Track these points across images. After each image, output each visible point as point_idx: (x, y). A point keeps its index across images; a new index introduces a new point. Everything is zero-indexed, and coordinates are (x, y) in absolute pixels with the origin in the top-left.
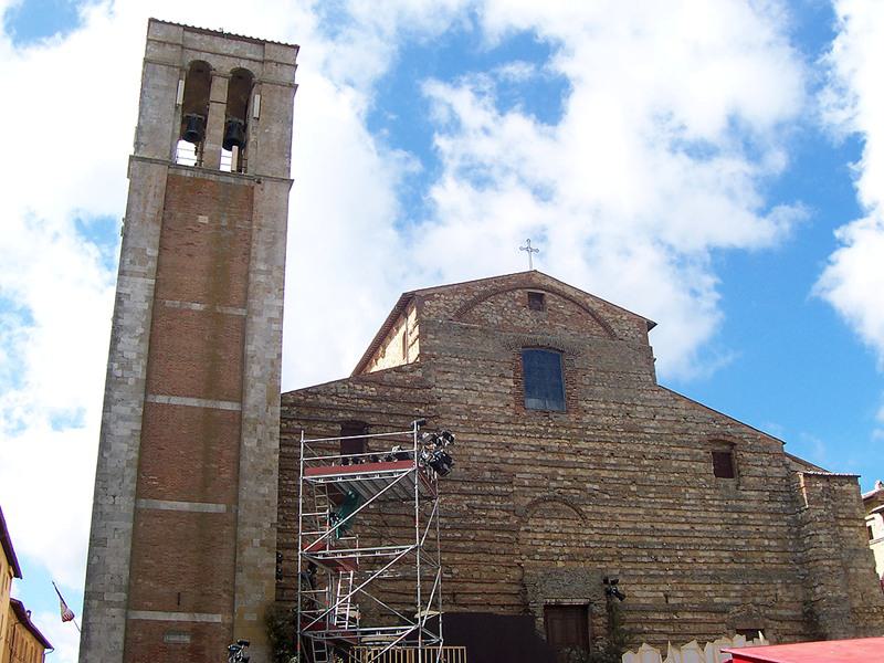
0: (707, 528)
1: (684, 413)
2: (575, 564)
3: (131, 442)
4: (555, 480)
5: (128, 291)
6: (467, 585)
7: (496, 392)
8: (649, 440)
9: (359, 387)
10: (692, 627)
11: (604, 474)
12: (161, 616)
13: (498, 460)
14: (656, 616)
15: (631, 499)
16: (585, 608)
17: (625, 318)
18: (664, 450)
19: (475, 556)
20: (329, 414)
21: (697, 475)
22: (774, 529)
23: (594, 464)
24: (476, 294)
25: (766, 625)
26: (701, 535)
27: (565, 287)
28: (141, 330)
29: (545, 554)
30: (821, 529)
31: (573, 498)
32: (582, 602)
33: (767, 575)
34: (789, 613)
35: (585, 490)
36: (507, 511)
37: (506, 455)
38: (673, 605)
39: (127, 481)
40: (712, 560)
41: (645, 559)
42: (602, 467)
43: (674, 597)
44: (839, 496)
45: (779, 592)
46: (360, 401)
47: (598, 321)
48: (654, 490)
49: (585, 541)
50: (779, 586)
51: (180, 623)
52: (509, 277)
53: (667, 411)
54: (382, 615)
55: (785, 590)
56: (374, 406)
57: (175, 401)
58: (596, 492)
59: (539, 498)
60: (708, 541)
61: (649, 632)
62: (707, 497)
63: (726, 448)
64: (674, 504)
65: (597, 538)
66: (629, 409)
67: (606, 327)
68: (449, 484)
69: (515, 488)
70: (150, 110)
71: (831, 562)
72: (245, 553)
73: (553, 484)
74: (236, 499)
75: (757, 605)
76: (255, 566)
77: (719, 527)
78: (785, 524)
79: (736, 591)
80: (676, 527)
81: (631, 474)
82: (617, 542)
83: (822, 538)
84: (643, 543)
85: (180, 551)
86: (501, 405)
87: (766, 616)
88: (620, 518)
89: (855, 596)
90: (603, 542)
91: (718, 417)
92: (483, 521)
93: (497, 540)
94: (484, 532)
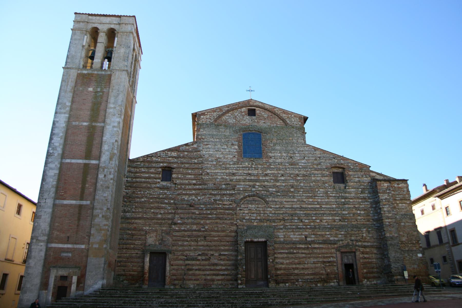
0: (328, 206)
1: (319, 156)
2: (262, 224)
3: (54, 178)
4: (254, 187)
5: (57, 120)
6: (212, 233)
7: (229, 151)
8: (301, 168)
9: (169, 153)
10: (318, 251)
11: (278, 184)
12: (61, 246)
13: (229, 180)
14: (301, 246)
15: (290, 195)
16: (265, 242)
17: (293, 116)
18: (308, 173)
19: (216, 221)
20: (157, 165)
21: (324, 183)
23: (273, 180)
24: (224, 111)
25: (356, 250)
26: (325, 209)
27: (265, 105)
28: (61, 134)
29: (248, 219)
30: (385, 205)
31: (262, 195)
32: (263, 240)
33: (357, 227)
34: (369, 244)
35: (268, 191)
36: (232, 201)
37: (232, 178)
38: (309, 241)
39: (51, 193)
40: (330, 221)
41: (296, 221)
42: (277, 181)
43: (310, 237)
44: (397, 189)
45: (364, 235)
46: (170, 159)
47: (280, 118)
48: (302, 190)
49: (267, 214)
51: (68, 248)
52: (239, 103)
53: (310, 155)
54: (173, 246)
55: (367, 233)
56: (176, 160)
57: (73, 161)
59: (247, 196)
60: (328, 212)
61: (297, 253)
62: (329, 193)
63: (340, 170)
64: (312, 196)
65: (273, 212)
66: (292, 155)
67: (284, 120)
70: (72, 49)
71: (390, 220)
72: (96, 220)
73: (254, 189)
74: (94, 199)
75: (352, 240)
76: (99, 225)
77: (334, 206)
78: (369, 203)
79: (341, 234)
80: (312, 206)
81: (291, 184)
82: (283, 214)
83: (385, 209)
84: (296, 214)
85: (70, 220)
86: (232, 157)
87: (357, 246)
88: (285, 203)
89: (404, 236)
90: (276, 214)
91: (335, 156)
92: (220, 206)
93: (226, 214)
94: (221, 211)
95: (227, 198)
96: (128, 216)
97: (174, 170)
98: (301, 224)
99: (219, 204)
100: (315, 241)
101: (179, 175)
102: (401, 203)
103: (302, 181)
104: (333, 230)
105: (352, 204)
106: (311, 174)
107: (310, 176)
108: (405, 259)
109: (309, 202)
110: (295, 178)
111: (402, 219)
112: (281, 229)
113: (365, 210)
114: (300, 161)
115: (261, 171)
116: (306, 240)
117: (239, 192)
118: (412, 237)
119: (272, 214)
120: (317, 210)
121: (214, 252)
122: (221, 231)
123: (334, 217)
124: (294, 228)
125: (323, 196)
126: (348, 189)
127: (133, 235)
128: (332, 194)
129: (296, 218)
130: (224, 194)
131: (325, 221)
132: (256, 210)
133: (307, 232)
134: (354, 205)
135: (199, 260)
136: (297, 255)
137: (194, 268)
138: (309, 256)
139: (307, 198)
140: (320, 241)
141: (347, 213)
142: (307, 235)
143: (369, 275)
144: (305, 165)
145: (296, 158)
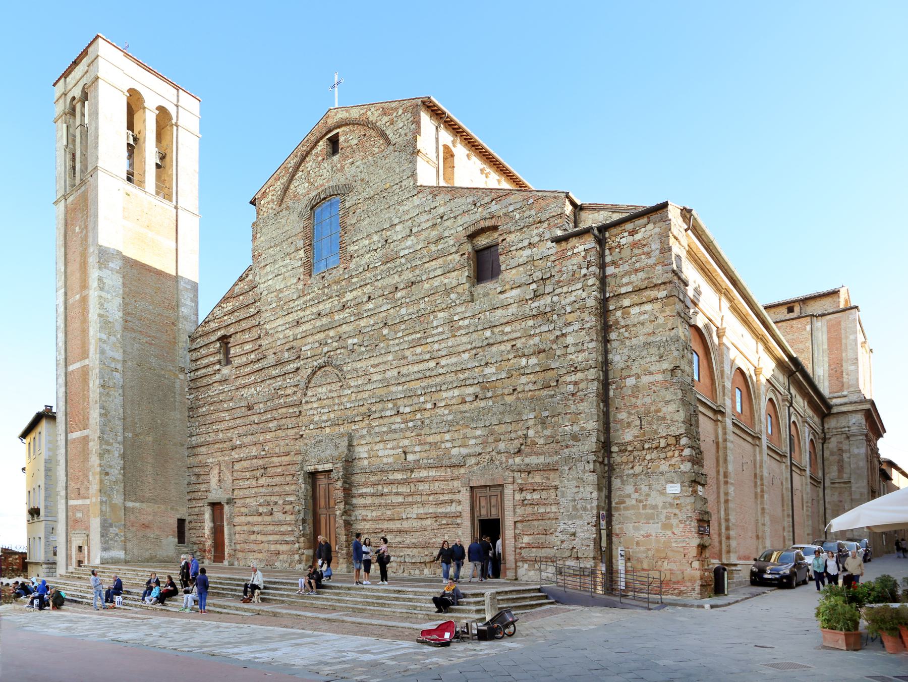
4: (326, 344)
11: (363, 323)
13: (291, 339)
18: (417, 272)
21: (448, 291)
22: (537, 339)
32: (328, 466)
40: (454, 401)
41: (388, 413)
48: (403, 327)
50: (531, 422)
58: (355, 347)
62: (456, 318)
65: (353, 396)
68: (266, 371)
69: (302, 362)
77: (466, 356)
79: (476, 437)
81: (384, 314)
87: (507, 468)
88: (372, 370)
95: (290, 379)
96: (194, 442)
97: (232, 340)
98: (398, 419)
99: (279, 397)
100: (421, 461)
101: (237, 347)
102: (637, 305)
103: (403, 300)
104: (458, 427)
108: (624, 502)
109: (415, 357)
110: (391, 296)
111: (629, 363)
112: (363, 437)
115: (337, 298)
116: (406, 459)
117: (305, 361)
118: (655, 427)
119: (351, 402)
120: (430, 377)
121: (278, 497)
122: (282, 454)
125: (443, 333)
126: (500, 293)
127: (199, 475)
129: (390, 405)
130: (285, 374)
131: (443, 404)
132: (328, 398)
134: (514, 343)
135: (261, 514)
136: (389, 499)
137: (256, 529)
138: (410, 499)
139: (411, 345)
140: (429, 461)
141: (494, 370)
142: (406, 447)
143: (534, 553)
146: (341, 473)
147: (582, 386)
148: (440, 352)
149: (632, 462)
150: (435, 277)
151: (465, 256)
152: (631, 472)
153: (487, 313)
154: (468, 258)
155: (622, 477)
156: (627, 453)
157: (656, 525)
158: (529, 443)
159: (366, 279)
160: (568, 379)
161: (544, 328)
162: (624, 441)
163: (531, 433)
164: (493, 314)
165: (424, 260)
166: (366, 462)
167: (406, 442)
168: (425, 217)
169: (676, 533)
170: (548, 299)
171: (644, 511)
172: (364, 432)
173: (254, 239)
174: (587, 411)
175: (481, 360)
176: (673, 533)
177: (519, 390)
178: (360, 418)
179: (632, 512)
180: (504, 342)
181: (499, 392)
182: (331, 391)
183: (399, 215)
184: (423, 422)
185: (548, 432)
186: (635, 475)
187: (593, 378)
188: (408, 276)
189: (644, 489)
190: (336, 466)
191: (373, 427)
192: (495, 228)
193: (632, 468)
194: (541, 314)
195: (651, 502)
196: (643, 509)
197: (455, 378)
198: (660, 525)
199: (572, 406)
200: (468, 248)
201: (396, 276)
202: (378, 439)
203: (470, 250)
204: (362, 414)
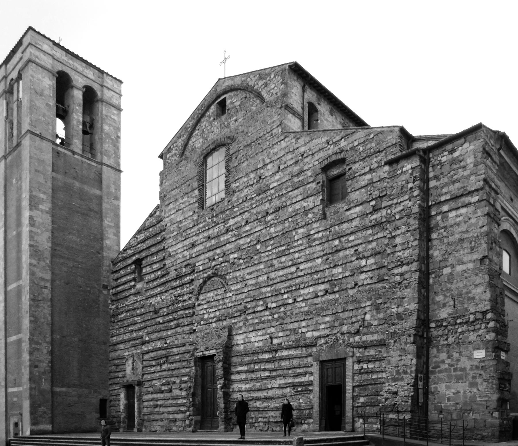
21: (306, 212)
22: (374, 244)
40: (309, 296)
41: (259, 309)
43: (277, 337)
50: (368, 309)
89: (444, 305)
98: (267, 313)
105: (351, 247)
106: (285, 202)
107: (284, 207)
108: (439, 367)
112: (240, 328)
113: (376, 254)
114: (273, 179)
116: (272, 343)
123: (316, 286)
124: (256, 323)
126: (347, 210)
128: (318, 232)
133: (273, 327)
134: (356, 248)
139: (278, 256)
142: (272, 333)
144: (280, 185)
145: (267, 175)
146: (222, 356)
147: (407, 276)
148: (299, 260)
149: (446, 335)
150: (297, 202)
151: (320, 185)
152: (445, 342)
153: (337, 227)
154: (323, 186)
155: (437, 347)
156: (443, 328)
157: (464, 384)
158: (366, 324)
159: (244, 208)
160: (396, 271)
161: (380, 235)
162: (440, 319)
163: (368, 317)
164: (341, 227)
165: (289, 190)
166: (242, 347)
167: (272, 330)
168: (290, 156)
169: (480, 389)
170: (384, 212)
171: (454, 373)
172: (241, 324)
173: (161, 184)
174: (410, 295)
175: (331, 263)
176: (478, 390)
177: (360, 284)
178: (238, 314)
179: (445, 374)
180: (349, 248)
181: (344, 287)
182: (217, 295)
183: (270, 157)
184: (285, 314)
185: (381, 316)
186: (448, 345)
187: (416, 269)
188: (277, 203)
189: (456, 355)
190: (218, 351)
191: (248, 320)
192: (342, 161)
193: (447, 339)
194: (379, 225)
195: (460, 365)
196: (454, 372)
197: (310, 278)
198: (467, 383)
199: (398, 293)
200: (321, 178)
201: (267, 204)
202: (251, 329)
203: (325, 179)
204: (240, 311)
